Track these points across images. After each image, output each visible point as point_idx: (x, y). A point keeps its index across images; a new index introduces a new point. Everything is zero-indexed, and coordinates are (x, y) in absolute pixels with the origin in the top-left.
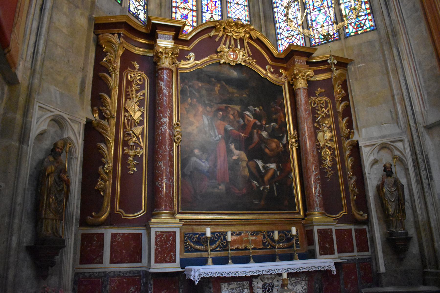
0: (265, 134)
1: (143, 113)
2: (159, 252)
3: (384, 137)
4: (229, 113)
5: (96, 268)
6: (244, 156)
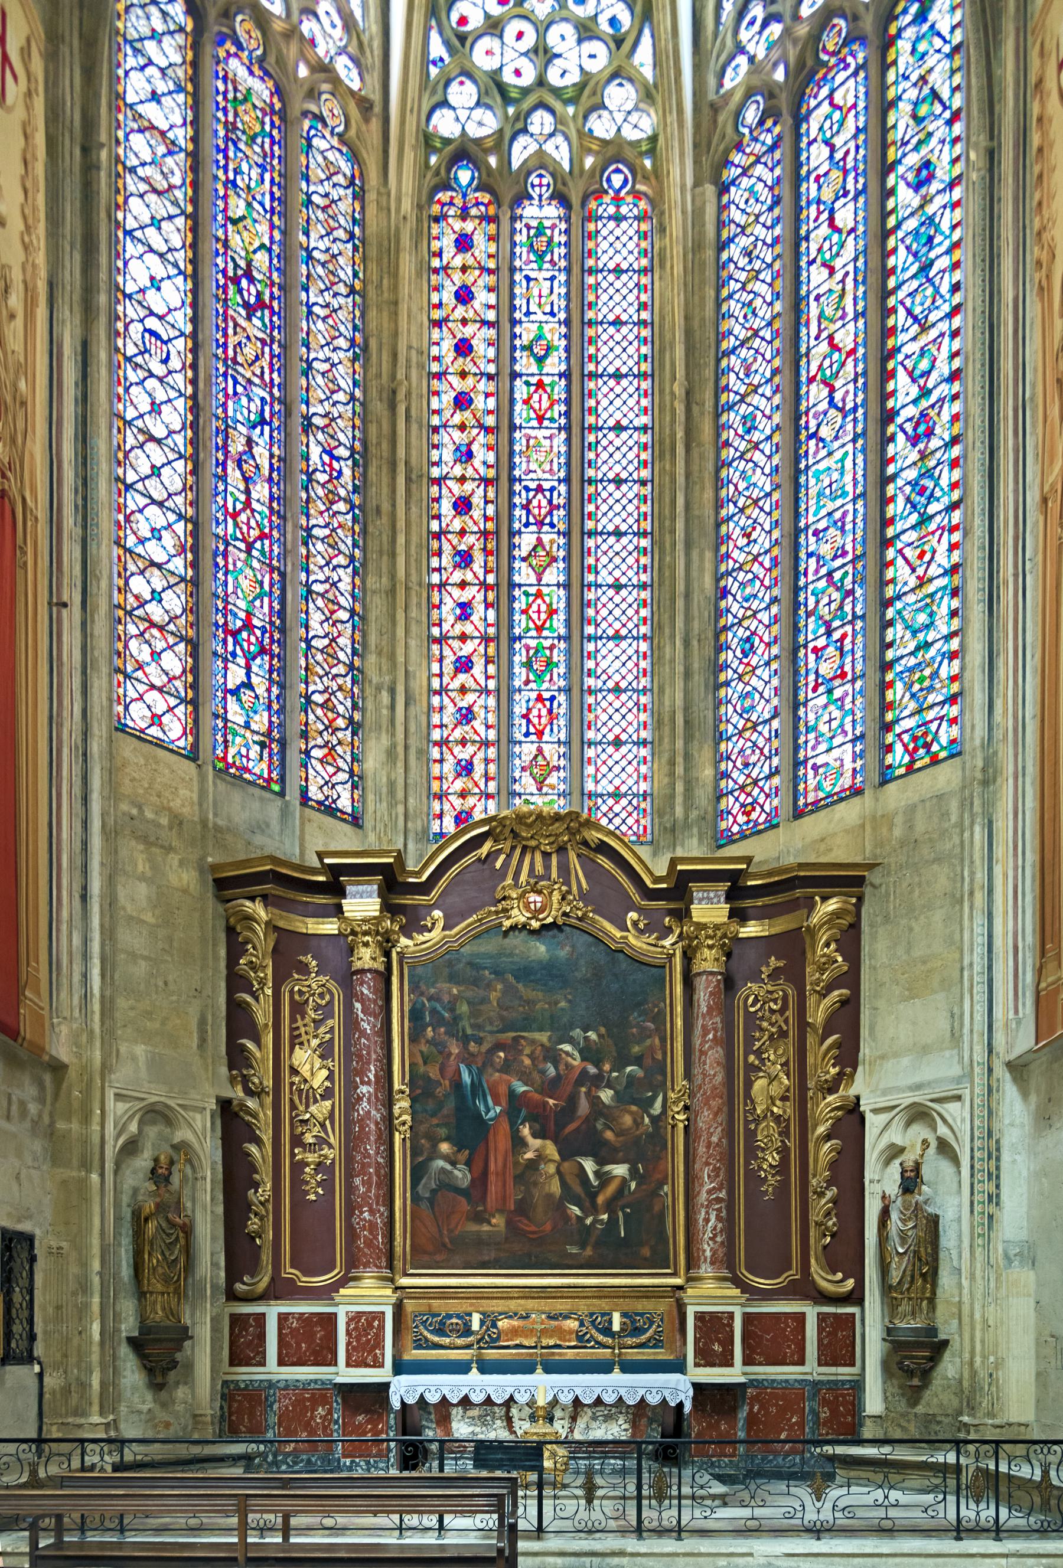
0: (606, 1095)
1: (331, 1072)
2: (354, 1349)
3: (918, 1087)
4: (521, 1052)
5: (247, 1374)
6: (551, 1150)
